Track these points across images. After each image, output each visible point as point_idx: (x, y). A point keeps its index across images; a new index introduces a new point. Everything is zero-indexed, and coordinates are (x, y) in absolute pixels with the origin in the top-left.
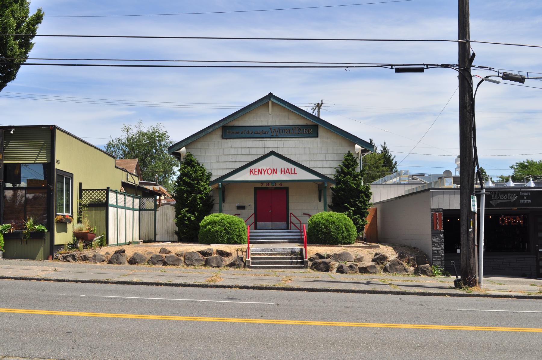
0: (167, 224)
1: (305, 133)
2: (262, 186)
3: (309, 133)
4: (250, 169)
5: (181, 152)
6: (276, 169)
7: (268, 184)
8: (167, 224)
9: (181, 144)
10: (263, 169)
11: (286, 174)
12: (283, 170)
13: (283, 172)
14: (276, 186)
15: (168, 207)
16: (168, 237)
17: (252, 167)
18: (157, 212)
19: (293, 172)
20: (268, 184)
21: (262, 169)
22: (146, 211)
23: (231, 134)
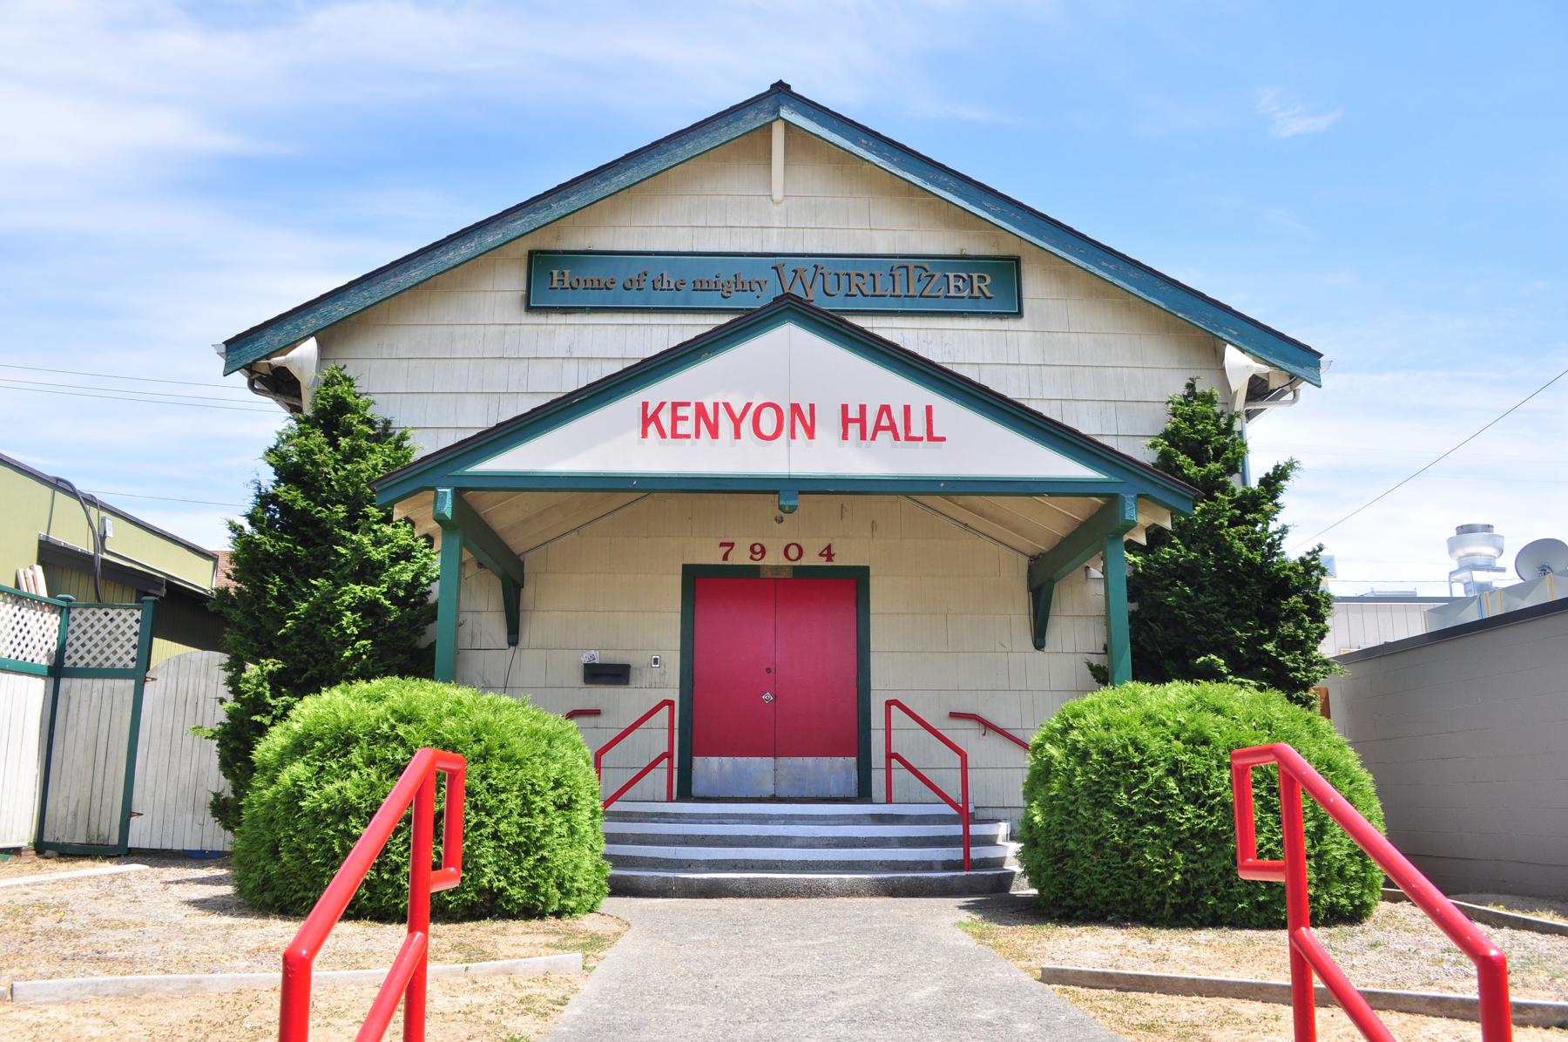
0: (196, 755)
1: (952, 293)
2: (725, 557)
3: (976, 293)
4: (645, 405)
5: (290, 361)
6: (812, 407)
7: (758, 549)
8: (196, 755)
9: (300, 322)
10: (727, 406)
11: (873, 438)
12: (854, 413)
13: (854, 429)
14: (804, 562)
15: (208, 660)
16: (196, 827)
17: (656, 393)
18: (148, 686)
19: (918, 428)
20: (758, 549)
21: (721, 408)
22: (85, 681)
23: (573, 288)
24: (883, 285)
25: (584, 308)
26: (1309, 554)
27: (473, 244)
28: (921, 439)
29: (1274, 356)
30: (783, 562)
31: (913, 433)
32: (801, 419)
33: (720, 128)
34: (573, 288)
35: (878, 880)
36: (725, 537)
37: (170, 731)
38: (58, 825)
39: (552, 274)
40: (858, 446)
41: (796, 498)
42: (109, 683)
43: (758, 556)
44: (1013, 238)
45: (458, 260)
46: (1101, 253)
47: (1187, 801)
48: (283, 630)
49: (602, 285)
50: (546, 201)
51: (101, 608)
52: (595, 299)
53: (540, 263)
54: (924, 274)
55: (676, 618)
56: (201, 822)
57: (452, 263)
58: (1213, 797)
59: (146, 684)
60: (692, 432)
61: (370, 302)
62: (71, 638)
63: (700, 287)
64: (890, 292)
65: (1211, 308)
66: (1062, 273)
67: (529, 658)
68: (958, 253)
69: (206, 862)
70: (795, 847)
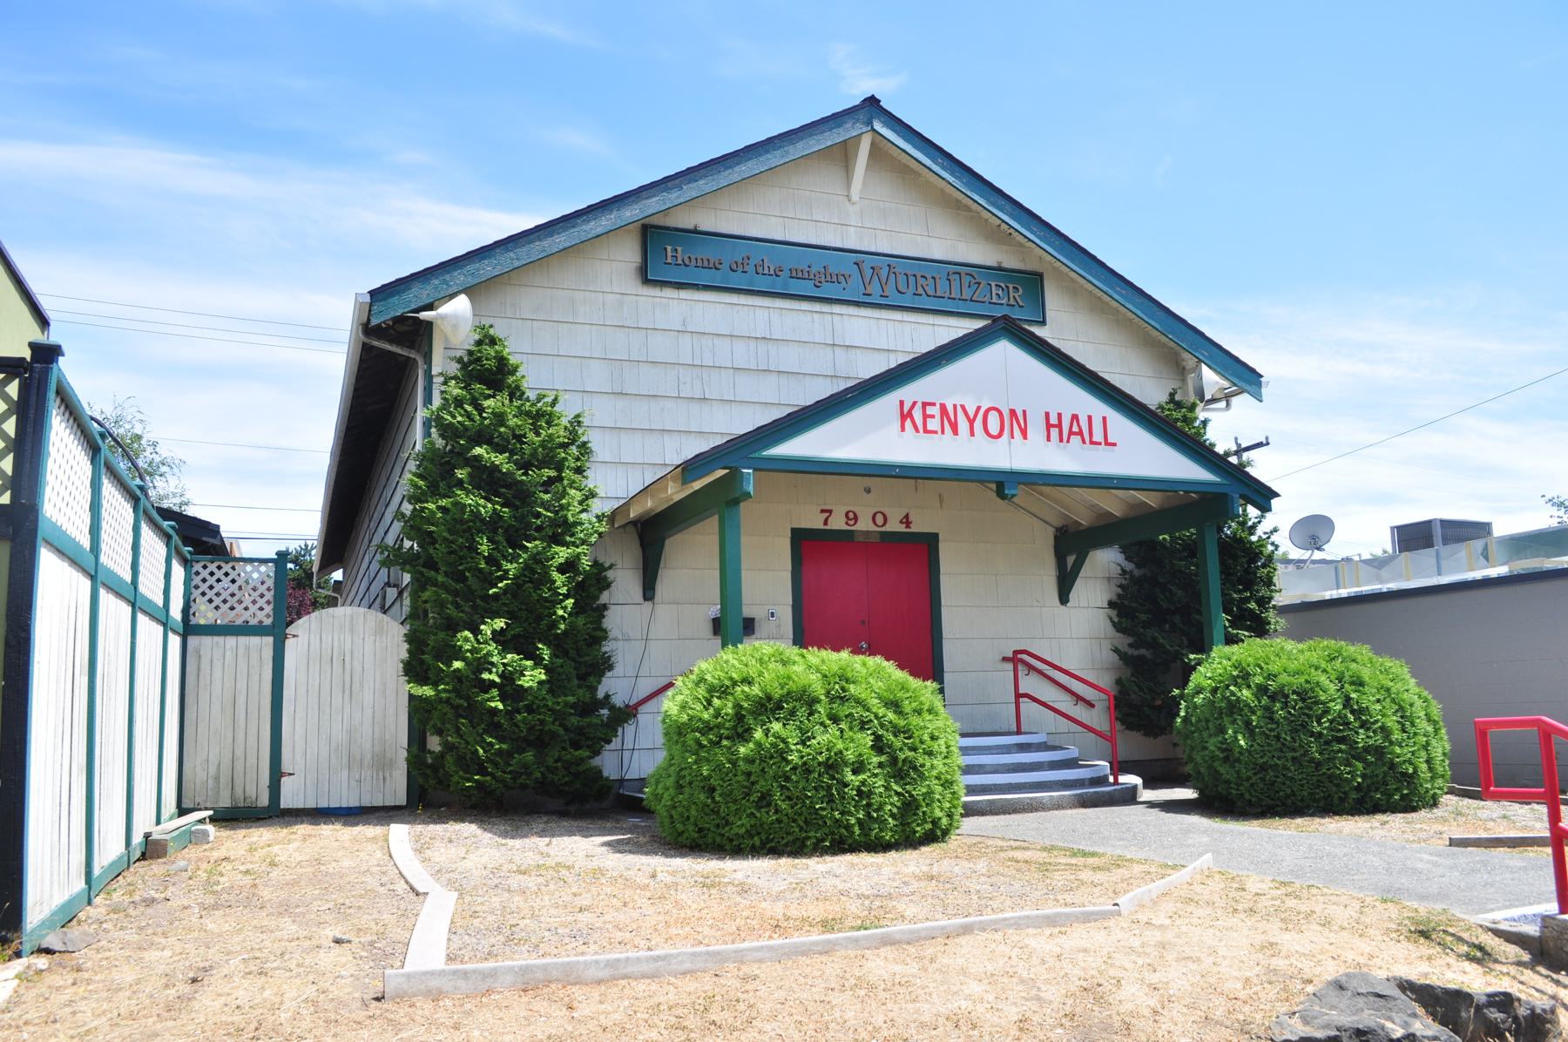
0: (347, 711)
1: (994, 300)
2: (826, 523)
3: (1012, 302)
4: (902, 403)
5: (443, 317)
6: (1024, 412)
7: (851, 515)
8: (347, 711)
9: (447, 277)
10: (963, 407)
11: (1068, 441)
12: (1054, 420)
13: (1054, 432)
14: (888, 528)
15: (352, 616)
16: (353, 784)
17: (911, 392)
18: (290, 644)
19: (1098, 437)
20: (851, 515)
21: (959, 408)
22: (216, 638)
23: (686, 265)
24: (942, 287)
25: (697, 285)
26: (1265, 533)
27: (612, 216)
28: (1100, 444)
29: (1231, 375)
30: (873, 528)
31: (1094, 439)
32: (1016, 421)
33: (824, 132)
34: (686, 265)
35: (1076, 795)
36: (825, 504)
37: (317, 689)
38: (198, 788)
39: (666, 249)
40: (1059, 447)
41: (1016, 488)
42: (243, 640)
43: (851, 522)
44: (1041, 256)
45: (600, 230)
46: (1115, 279)
47: (1361, 727)
48: (494, 590)
49: (711, 265)
50: (677, 181)
51: (227, 563)
52: (705, 277)
53: (652, 236)
54: (973, 281)
55: (788, 576)
56: (357, 777)
57: (594, 233)
58: (1377, 721)
59: (287, 641)
60: (938, 428)
61: (517, 264)
62: (196, 593)
63: (796, 275)
64: (947, 295)
65: (1190, 332)
66: (1073, 291)
67: (664, 610)
68: (996, 265)
69: (351, 819)
70: (986, 773)
